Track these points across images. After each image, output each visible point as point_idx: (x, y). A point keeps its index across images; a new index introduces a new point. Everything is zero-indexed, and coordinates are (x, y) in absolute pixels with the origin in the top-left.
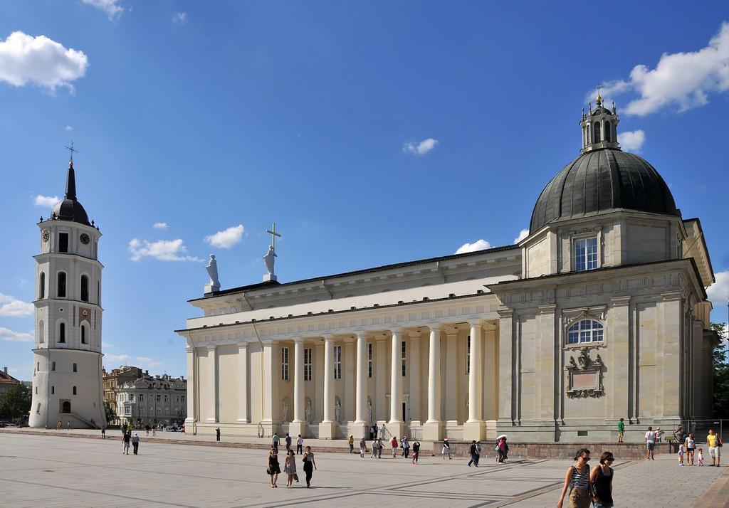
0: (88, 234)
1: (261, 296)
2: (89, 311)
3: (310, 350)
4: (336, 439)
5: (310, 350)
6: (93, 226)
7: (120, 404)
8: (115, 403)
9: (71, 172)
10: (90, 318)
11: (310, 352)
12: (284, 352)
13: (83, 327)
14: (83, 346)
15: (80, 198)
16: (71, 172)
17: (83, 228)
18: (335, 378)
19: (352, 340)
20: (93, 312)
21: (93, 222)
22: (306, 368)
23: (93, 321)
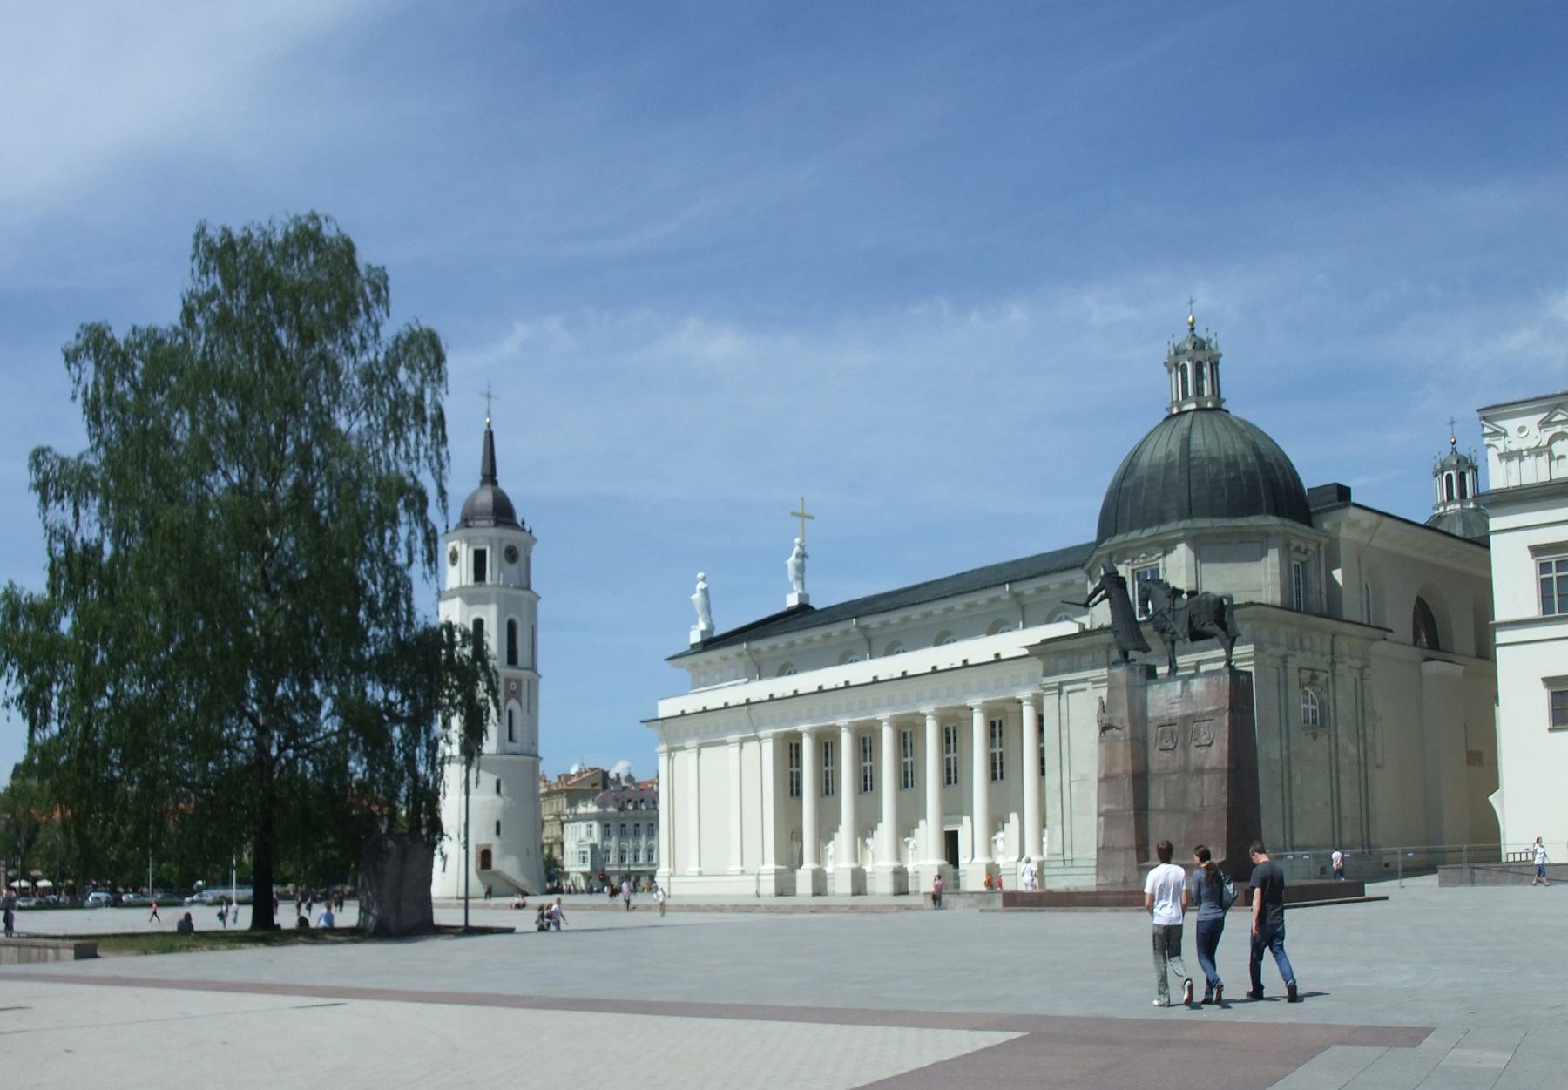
0: (516, 545)
1: (770, 647)
2: (519, 682)
3: (1000, 722)
4: (781, 895)
5: (1000, 722)
6: (524, 530)
7: (570, 845)
8: (562, 844)
9: (490, 436)
10: (521, 694)
11: (1000, 726)
12: (790, 749)
13: (510, 713)
14: (511, 747)
15: (505, 483)
16: (490, 436)
17: (508, 535)
18: (792, 794)
19: (1016, 706)
20: (525, 684)
21: (523, 523)
22: (993, 755)
23: (524, 699)
